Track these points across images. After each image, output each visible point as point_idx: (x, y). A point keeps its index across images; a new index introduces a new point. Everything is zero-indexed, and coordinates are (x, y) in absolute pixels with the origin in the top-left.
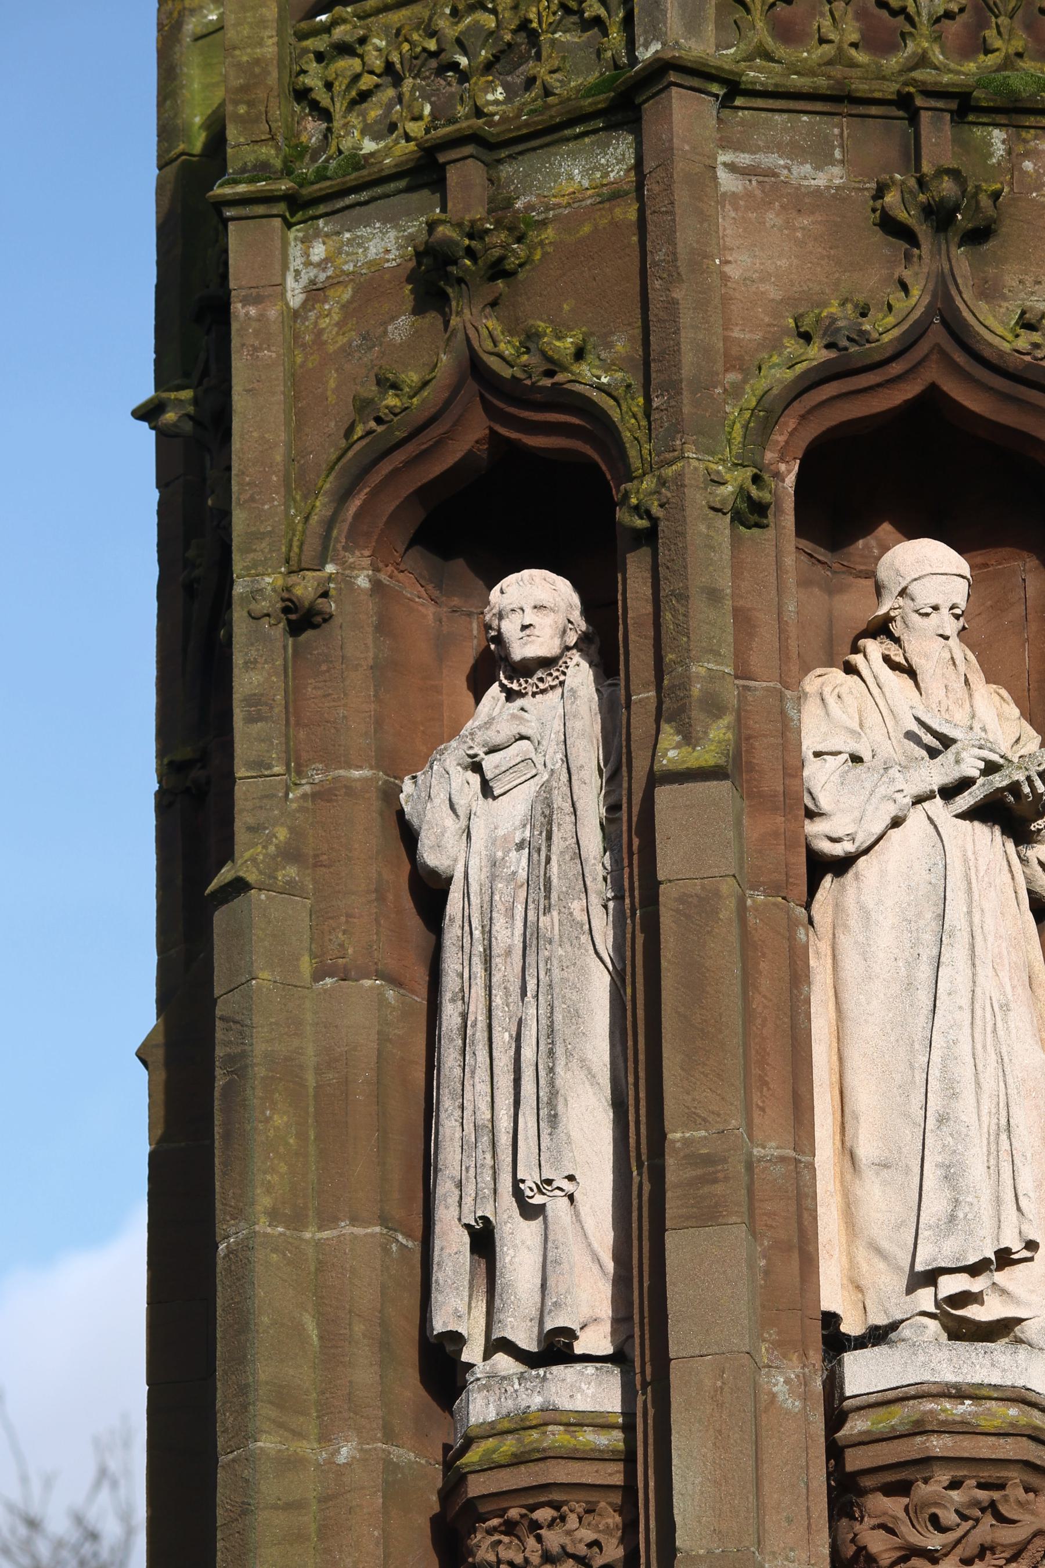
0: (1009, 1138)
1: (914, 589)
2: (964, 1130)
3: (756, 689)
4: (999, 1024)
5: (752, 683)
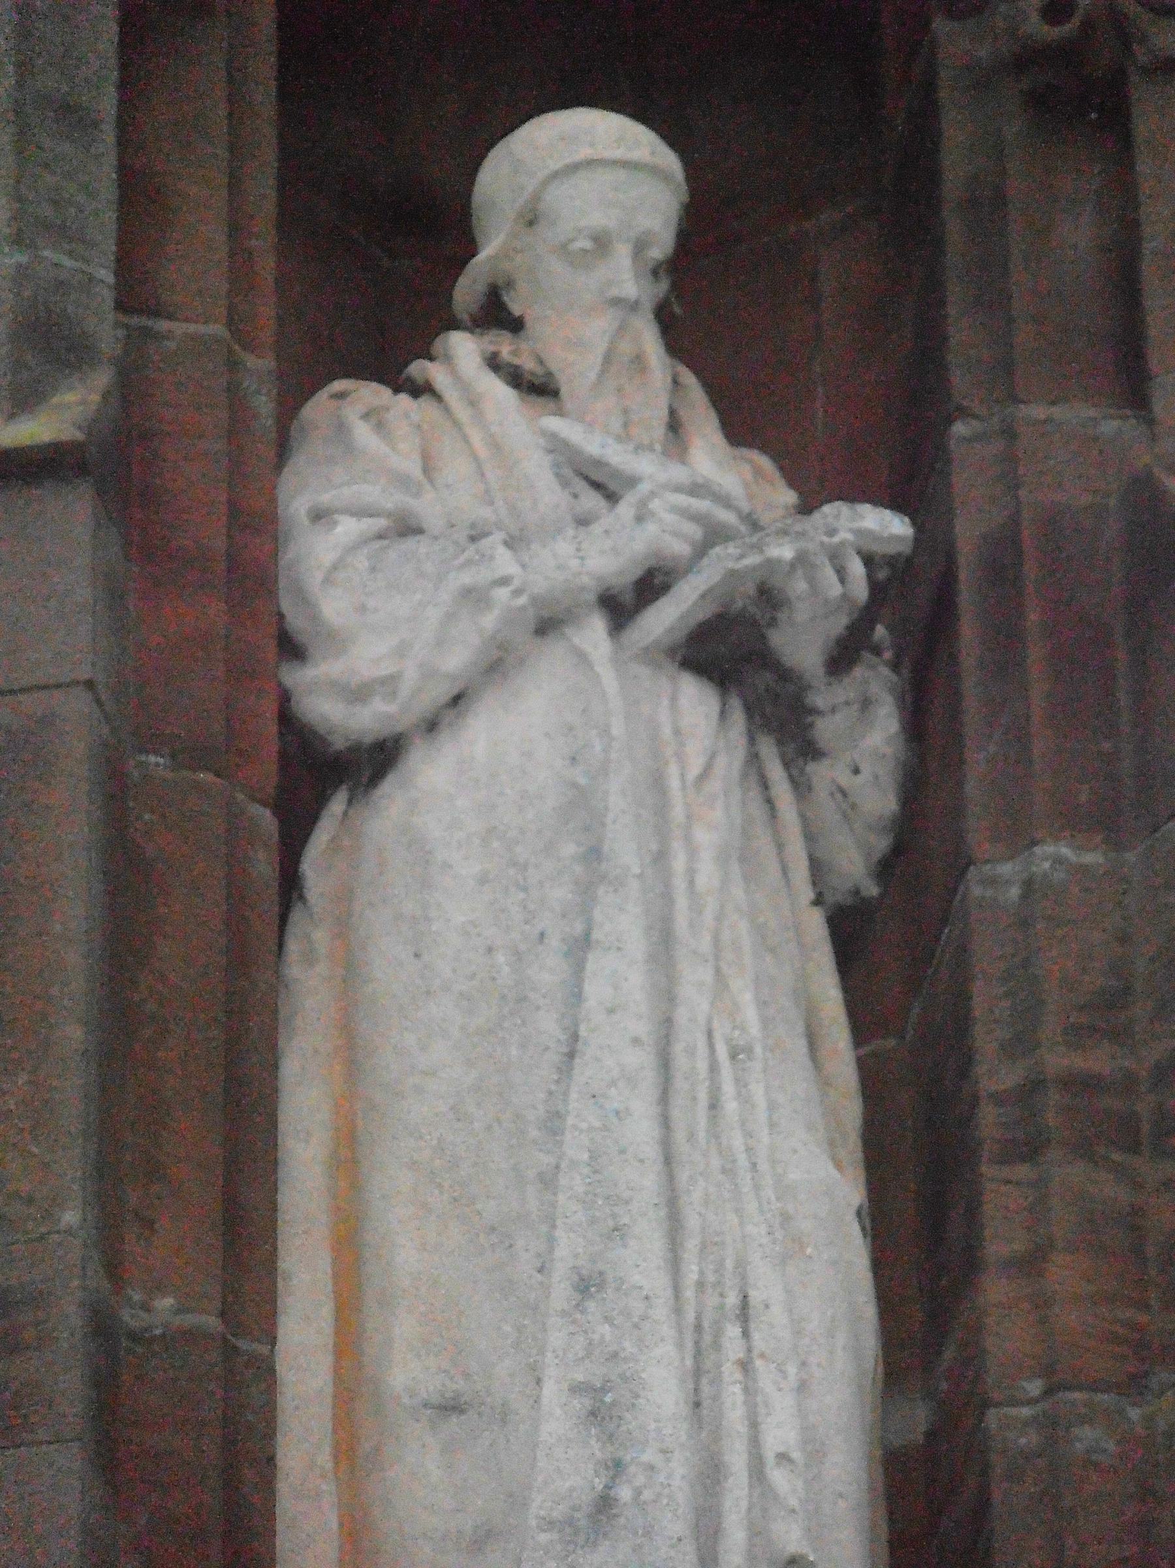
0: (746, 1334)
1: (560, 197)
2: (638, 1307)
3: (169, 335)
4: (728, 1088)
5: (163, 325)
